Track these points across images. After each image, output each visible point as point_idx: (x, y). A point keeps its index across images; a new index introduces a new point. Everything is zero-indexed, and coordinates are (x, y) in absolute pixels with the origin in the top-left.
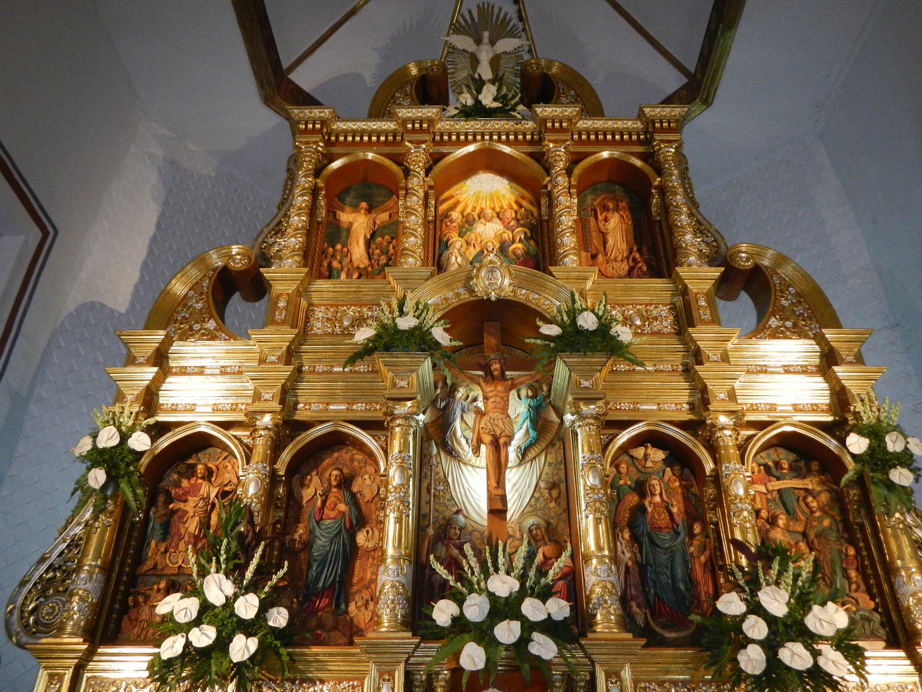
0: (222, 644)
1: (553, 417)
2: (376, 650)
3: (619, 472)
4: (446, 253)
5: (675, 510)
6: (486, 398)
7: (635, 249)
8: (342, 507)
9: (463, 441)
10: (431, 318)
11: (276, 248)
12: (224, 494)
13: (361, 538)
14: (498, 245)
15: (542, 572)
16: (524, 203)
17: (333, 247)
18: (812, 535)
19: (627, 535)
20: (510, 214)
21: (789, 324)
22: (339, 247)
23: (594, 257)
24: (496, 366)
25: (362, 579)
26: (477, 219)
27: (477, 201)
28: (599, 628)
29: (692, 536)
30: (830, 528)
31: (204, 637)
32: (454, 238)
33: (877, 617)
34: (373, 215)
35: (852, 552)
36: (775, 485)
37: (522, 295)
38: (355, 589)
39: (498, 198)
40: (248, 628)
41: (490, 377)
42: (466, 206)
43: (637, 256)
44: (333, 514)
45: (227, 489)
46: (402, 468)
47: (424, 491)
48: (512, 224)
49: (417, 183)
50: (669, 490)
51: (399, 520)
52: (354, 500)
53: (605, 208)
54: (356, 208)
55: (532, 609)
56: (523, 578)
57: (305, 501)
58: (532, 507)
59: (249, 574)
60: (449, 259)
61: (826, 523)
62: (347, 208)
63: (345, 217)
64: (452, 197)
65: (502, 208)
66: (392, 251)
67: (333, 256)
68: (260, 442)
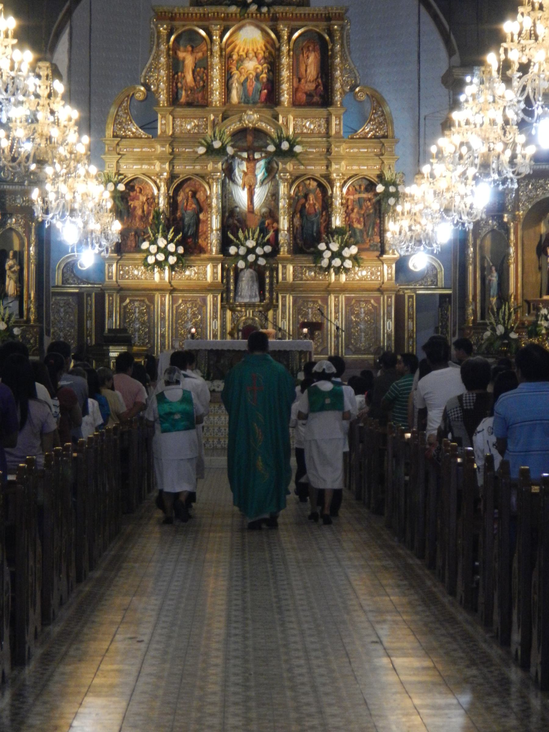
0: (166, 259)
1: (275, 166)
2: (211, 260)
3: (299, 190)
4: (230, 82)
5: (316, 207)
6: (247, 168)
7: (319, 76)
8: (194, 206)
9: (239, 178)
10: (226, 139)
11: (152, 80)
12: (148, 199)
13: (201, 216)
14: (254, 74)
15: (264, 237)
16: (269, 47)
17: (177, 73)
18: (365, 215)
19: (298, 215)
20: (260, 56)
21: (375, 127)
22: (180, 74)
23: (300, 80)
24: (251, 156)
25: (202, 231)
26: (245, 56)
27: (245, 45)
28: (281, 253)
29: (322, 216)
30: (372, 213)
31: (161, 257)
32: (234, 71)
33: (379, 244)
34: (195, 54)
35: (378, 221)
36: (357, 196)
37: (263, 125)
38: (200, 234)
39: (255, 42)
40: (172, 254)
41: (248, 160)
42: (240, 48)
43: (320, 81)
44: (191, 208)
45: (149, 197)
46: (217, 198)
47: (224, 198)
48: (262, 61)
49: (216, 48)
50: (316, 198)
51: (216, 218)
52: (198, 202)
53: (308, 50)
54: (185, 51)
55: (259, 251)
56: (257, 240)
57: (179, 202)
58: (265, 204)
59: (170, 236)
60: (232, 84)
61: (371, 211)
62: (182, 48)
63: (181, 55)
64: (232, 42)
65: (257, 50)
66: (205, 78)
67: (178, 78)
68: (162, 184)
